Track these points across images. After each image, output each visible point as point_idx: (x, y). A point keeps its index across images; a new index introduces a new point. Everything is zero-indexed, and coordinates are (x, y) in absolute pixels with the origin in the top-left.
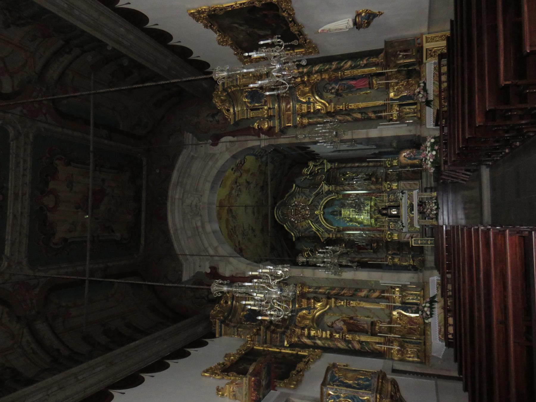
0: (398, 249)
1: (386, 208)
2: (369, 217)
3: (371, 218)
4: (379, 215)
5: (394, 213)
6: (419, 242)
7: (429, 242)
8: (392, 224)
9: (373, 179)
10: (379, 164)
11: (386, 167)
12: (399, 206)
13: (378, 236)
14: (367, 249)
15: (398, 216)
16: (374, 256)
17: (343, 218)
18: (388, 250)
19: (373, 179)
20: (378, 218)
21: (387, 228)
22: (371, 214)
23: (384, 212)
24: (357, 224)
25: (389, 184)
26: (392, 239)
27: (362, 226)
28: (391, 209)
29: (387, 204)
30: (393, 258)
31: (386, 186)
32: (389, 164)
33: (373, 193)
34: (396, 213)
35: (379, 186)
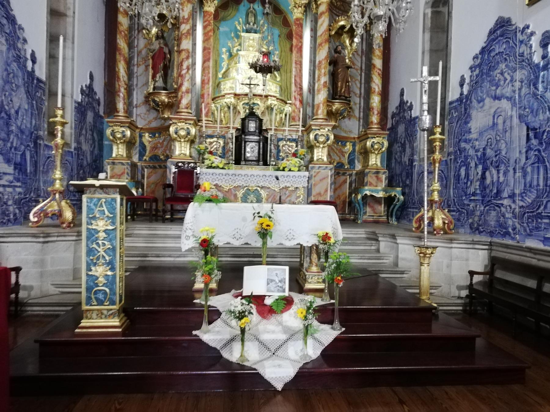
0: (155, 158)
1: (261, 131)
2: (238, 92)
3: (236, 95)
4: (242, 115)
5: (248, 149)
6: (101, 225)
7: (100, 271)
8: (217, 144)
9: (337, 106)
10: (375, 119)
11: (363, 137)
12: (266, 164)
13: (184, 102)
14: (154, 77)
15: (239, 158)
16: (138, 97)
17: (238, 37)
18: (153, 132)
19: (337, 106)
20: (236, 111)
21: (210, 132)
22: (246, 95)
23: (252, 126)
24: (224, 70)
25: (328, 139)
26: (174, 140)
27: (215, 76)
28: (259, 142)
29: (271, 133)
30: (130, 144)
31: (325, 131)
32: (372, 146)
33: (301, 102)
34: (248, 155)
35: (321, 112)
